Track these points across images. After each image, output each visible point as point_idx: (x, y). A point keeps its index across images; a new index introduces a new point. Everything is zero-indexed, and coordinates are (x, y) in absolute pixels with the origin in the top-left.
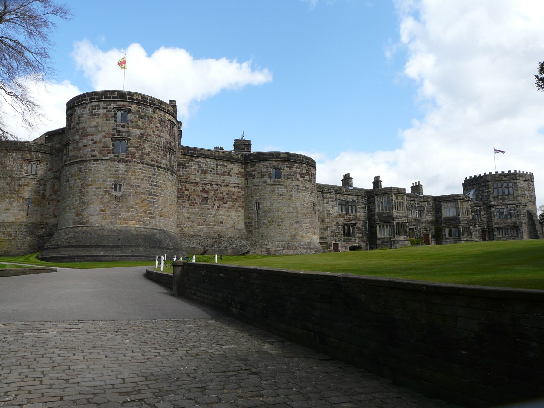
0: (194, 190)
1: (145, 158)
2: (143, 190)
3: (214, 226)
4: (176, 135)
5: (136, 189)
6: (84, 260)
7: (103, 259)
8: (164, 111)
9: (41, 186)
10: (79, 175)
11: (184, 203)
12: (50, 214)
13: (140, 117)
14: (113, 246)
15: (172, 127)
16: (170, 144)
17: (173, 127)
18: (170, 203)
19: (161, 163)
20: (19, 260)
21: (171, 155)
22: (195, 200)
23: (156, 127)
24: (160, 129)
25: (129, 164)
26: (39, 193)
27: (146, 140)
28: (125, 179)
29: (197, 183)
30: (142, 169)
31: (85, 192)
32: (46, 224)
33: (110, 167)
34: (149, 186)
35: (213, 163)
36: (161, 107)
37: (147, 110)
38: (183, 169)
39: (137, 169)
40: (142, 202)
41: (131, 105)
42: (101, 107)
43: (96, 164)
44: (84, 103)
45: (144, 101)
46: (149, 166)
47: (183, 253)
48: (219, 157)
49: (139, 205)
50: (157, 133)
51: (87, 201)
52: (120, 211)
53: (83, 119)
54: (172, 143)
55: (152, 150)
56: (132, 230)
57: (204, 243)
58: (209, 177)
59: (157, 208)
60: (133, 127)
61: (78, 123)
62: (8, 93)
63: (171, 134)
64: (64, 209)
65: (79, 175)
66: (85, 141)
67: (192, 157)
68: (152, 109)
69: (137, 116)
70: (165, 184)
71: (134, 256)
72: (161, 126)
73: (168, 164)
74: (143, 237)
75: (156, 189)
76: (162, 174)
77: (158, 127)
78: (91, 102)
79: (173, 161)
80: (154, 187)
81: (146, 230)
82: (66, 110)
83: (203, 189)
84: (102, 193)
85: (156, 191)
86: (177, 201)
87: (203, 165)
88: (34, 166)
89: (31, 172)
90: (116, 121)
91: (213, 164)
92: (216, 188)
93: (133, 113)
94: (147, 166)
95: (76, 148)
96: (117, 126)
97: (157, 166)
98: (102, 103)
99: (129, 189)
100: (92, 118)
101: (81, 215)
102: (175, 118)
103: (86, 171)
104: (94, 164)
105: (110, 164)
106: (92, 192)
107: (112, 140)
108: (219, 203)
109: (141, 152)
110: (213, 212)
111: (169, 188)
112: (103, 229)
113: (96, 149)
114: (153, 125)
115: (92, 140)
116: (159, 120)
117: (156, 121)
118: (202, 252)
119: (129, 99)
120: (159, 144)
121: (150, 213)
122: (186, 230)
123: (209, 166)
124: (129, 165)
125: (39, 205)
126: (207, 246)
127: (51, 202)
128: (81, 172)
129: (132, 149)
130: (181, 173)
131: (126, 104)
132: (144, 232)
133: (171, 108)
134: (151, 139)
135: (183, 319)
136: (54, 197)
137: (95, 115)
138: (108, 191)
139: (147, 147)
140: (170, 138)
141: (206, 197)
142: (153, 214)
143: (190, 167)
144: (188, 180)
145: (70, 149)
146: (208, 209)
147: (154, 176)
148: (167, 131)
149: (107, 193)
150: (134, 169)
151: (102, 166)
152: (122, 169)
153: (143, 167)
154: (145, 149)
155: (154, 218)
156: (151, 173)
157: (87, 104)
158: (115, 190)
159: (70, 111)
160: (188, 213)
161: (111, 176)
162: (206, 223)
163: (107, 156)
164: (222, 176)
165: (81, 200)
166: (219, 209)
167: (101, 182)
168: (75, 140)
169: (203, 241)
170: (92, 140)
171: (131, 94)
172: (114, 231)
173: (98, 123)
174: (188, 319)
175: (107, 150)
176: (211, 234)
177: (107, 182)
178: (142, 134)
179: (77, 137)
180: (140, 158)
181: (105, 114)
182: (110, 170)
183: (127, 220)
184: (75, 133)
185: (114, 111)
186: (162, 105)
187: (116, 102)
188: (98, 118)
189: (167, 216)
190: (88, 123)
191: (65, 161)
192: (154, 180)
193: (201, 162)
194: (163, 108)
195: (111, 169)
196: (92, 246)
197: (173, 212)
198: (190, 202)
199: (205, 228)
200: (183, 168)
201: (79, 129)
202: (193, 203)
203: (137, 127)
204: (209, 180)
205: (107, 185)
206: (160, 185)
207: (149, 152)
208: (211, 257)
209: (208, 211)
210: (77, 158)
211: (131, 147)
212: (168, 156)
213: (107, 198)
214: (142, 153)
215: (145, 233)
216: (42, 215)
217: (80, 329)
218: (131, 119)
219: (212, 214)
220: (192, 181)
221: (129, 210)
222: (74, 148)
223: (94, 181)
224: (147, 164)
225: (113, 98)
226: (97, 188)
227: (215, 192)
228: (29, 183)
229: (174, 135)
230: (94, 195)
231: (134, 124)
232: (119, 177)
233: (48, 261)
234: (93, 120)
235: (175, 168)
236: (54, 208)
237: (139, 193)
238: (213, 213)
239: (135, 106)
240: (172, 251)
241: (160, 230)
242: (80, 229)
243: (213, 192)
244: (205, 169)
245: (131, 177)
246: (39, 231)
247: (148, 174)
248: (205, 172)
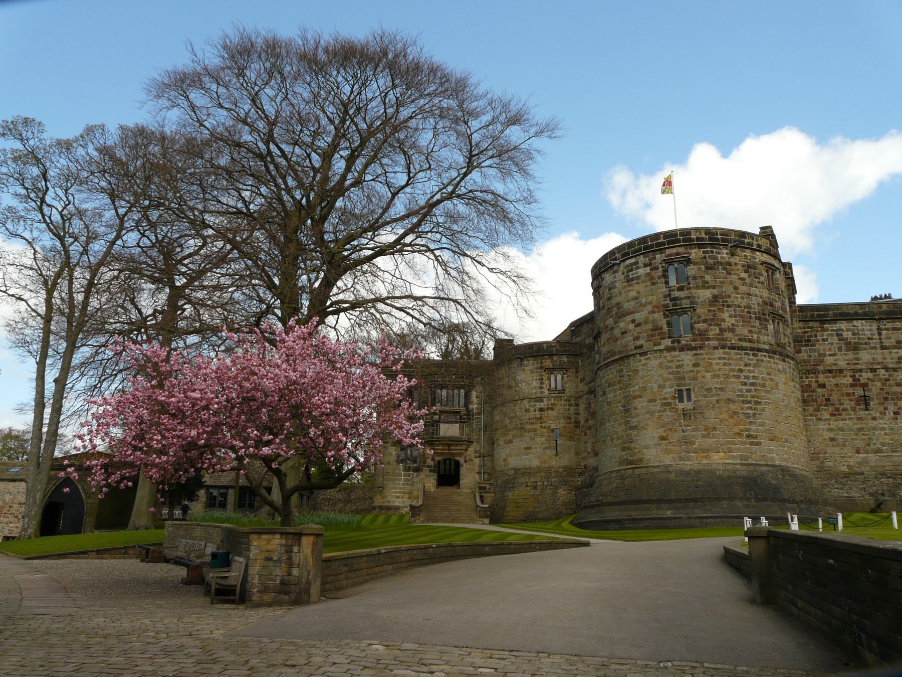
0: (837, 385)
1: (727, 338)
2: (730, 395)
3: (893, 452)
4: (783, 285)
5: (718, 395)
6: (641, 525)
7: (672, 524)
8: (751, 249)
9: (572, 408)
10: (619, 382)
11: (819, 411)
12: (589, 450)
13: (707, 268)
14: (688, 500)
15: (770, 274)
16: (771, 305)
17: (773, 273)
18: (788, 414)
19: (758, 342)
20: (548, 526)
21: (776, 324)
22: (841, 404)
23: (740, 279)
24: (747, 281)
25: (699, 352)
26: (570, 418)
27: (723, 306)
28: (695, 379)
29: (841, 371)
30: (725, 358)
31: (632, 410)
32: (585, 467)
33: (668, 362)
34: (741, 387)
35: (868, 328)
36: (743, 242)
37: (719, 253)
38: (808, 348)
39: (714, 359)
40: (731, 417)
41: (689, 250)
42: (641, 264)
43: (643, 360)
44: (614, 264)
45: (710, 239)
46: (736, 351)
47: (827, 510)
48: (881, 313)
49: (726, 423)
50: (743, 289)
51: (636, 424)
52: (693, 436)
53: (616, 290)
54: (776, 301)
55: (737, 321)
56: (719, 470)
57: (875, 488)
58: (865, 356)
59: (762, 425)
60: (697, 288)
61: (609, 299)
62: (492, 269)
63: (772, 287)
64: (604, 441)
65: (619, 382)
66: (622, 325)
67: (823, 322)
68: (727, 249)
69: (703, 267)
70: (772, 380)
71: (727, 517)
72: (749, 276)
73: (773, 343)
74: (740, 480)
75: (756, 390)
76: (762, 361)
77: (743, 279)
78: (624, 261)
79: (782, 336)
80: (750, 388)
81: (744, 467)
82: (591, 281)
83: (856, 380)
84: (658, 407)
85: (755, 394)
86: (804, 410)
87: (847, 335)
88: (559, 377)
89: (556, 387)
90: (667, 283)
91: (870, 330)
92: (884, 375)
93: (695, 264)
94: (732, 351)
95: (611, 338)
96: (670, 291)
97: (752, 349)
98: (642, 257)
99: (706, 396)
100: (629, 286)
101: (629, 448)
102: (777, 257)
103: (630, 373)
104: (640, 361)
105: (666, 357)
106: (643, 407)
107: (665, 316)
108: (896, 404)
109: (718, 328)
110: (886, 424)
111: (781, 386)
112: (667, 469)
113: (641, 335)
114: (734, 277)
115: (633, 321)
116: (743, 266)
117: (738, 269)
118: (873, 506)
119: (684, 240)
120: (750, 308)
121: (749, 436)
122: (831, 464)
123: (862, 335)
124: (700, 354)
125: (571, 438)
126: (883, 495)
127: (588, 432)
128: (622, 376)
129: (702, 324)
130: (804, 355)
131: (681, 250)
132: (743, 471)
133: (764, 240)
134: (733, 302)
135: (733, 667)
136: (591, 422)
137: (633, 279)
138: (669, 404)
139: (727, 318)
140: (771, 294)
141: (865, 396)
142: (756, 437)
143: (821, 342)
144: (821, 368)
145: (603, 342)
146: (874, 419)
147: (748, 368)
148: (763, 283)
149: (668, 408)
150: (709, 359)
151: (654, 362)
152: (688, 362)
153: (724, 353)
154: (725, 322)
155: (758, 444)
156: (742, 363)
157: (619, 264)
158: (681, 401)
159: (596, 282)
160: (830, 430)
161: (670, 376)
162: (872, 447)
163: (660, 344)
164: (894, 351)
165: (627, 423)
166: (899, 417)
167: (656, 390)
168: (607, 327)
169: (871, 483)
170: (633, 321)
171: (686, 232)
172: (687, 473)
173: (638, 292)
174: (747, 666)
175: (659, 334)
176: (887, 468)
177: (665, 388)
178: (715, 297)
179: (610, 321)
180: (718, 339)
181: (648, 275)
182: (668, 368)
183: (708, 453)
184: (607, 314)
185: (663, 267)
186: (745, 238)
187: (663, 251)
188: (638, 283)
189: (784, 440)
190: (623, 295)
191: (599, 363)
192: (749, 374)
193: (842, 330)
194: (749, 244)
195: (669, 365)
196: (650, 501)
197: (797, 430)
198: (831, 409)
199: (872, 457)
200: (807, 346)
201: (612, 308)
202: (837, 409)
203: (705, 285)
204: (866, 361)
205: (665, 393)
206: (762, 382)
207: (733, 325)
208: (885, 514)
209: (873, 424)
210: (614, 354)
211: (698, 322)
212: (770, 327)
213: (668, 416)
214: (720, 330)
215: (745, 473)
216: (577, 454)
217: (496, 669)
218: (694, 273)
219: (883, 429)
220: (830, 368)
221: (709, 433)
222: (608, 340)
223: (644, 389)
224: (733, 348)
225: (658, 245)
226: (651, 401)
227: (884, 384)
228: (554, 405)
229: (778, 288)
230: (648, 413)
231: (699, 281)
232: (684, 378)
233: (587, 529)
234: (630, 288)
235: (788, 348)
236: (593, 440)
237: (723, 402)
238: (886, 426)
239: (696, 250)
240: (803, 506)
241: (774, 466)
242: (630, 472)
243: (879, 385)
244: (853, 341)
245: (706, 374)
246: (576, 480)
247: (735, 365)
248: (855, 348)
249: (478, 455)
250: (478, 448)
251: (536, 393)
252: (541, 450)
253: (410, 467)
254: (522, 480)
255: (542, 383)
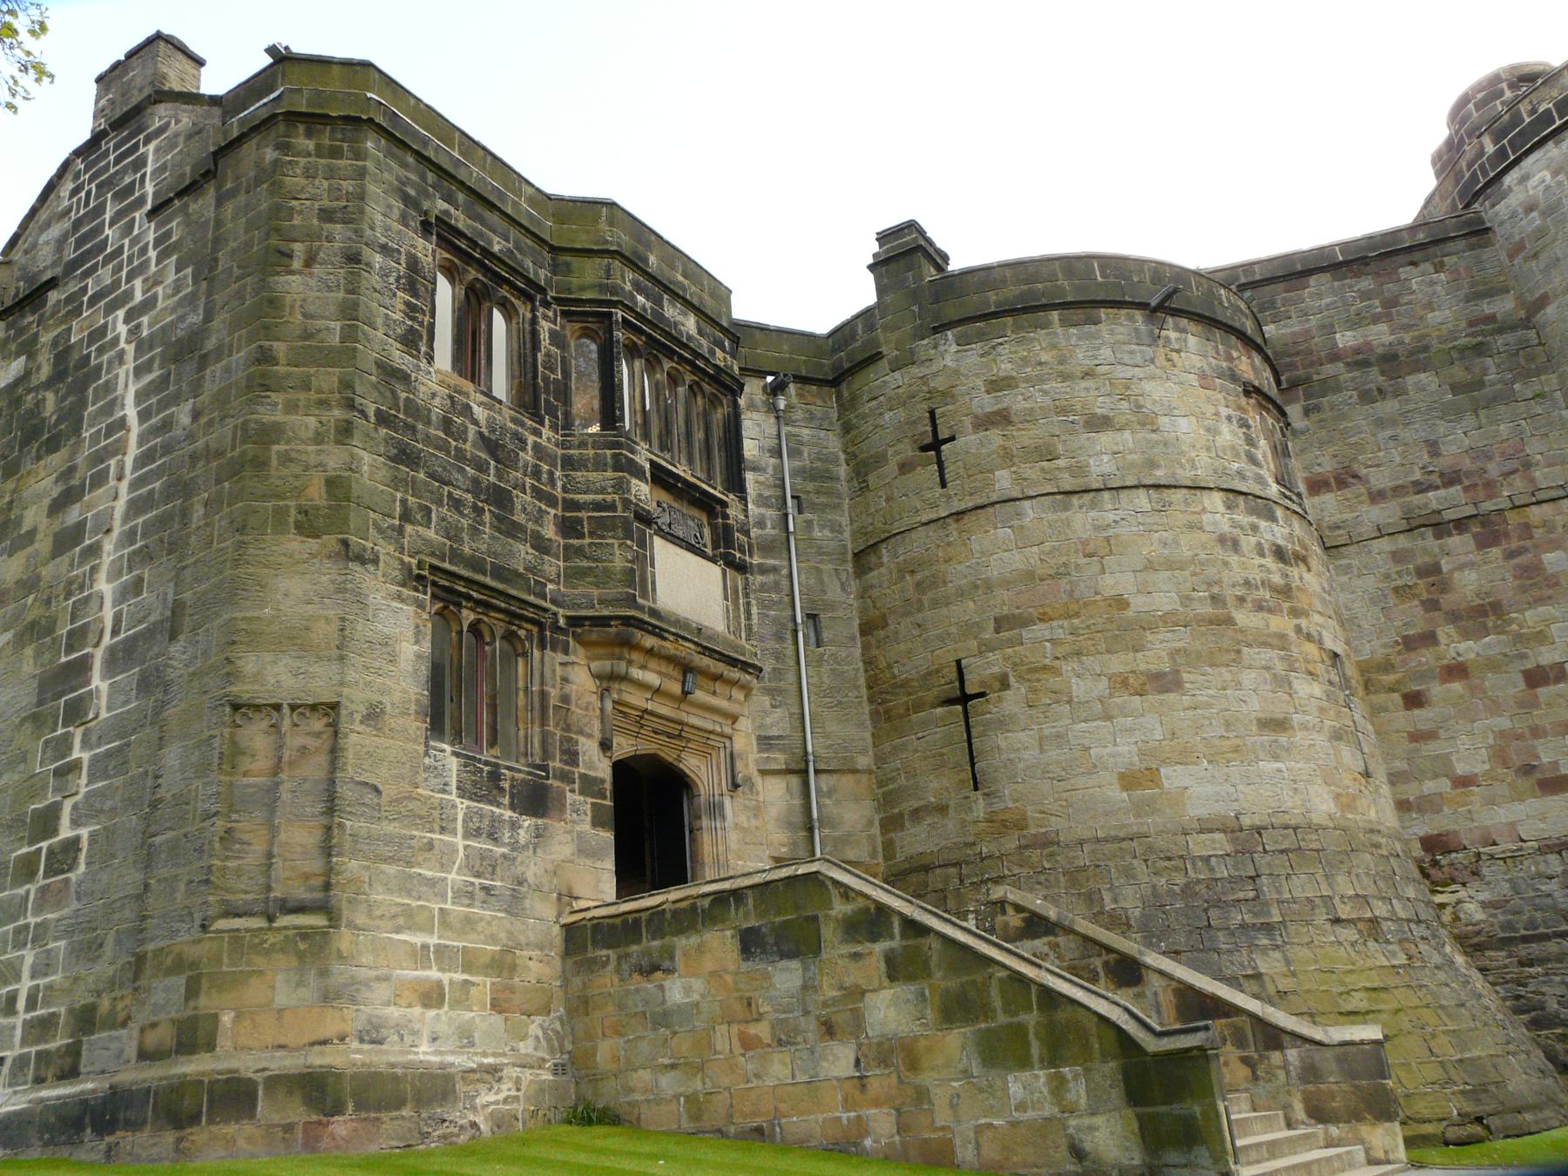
127: (1436, 690)
136: (1457, 646)
236: (1504, 723)
249: (779, 759)
250: (778, 722)
251: (1241, 475)
252: (1321, 740)
253: (495, 776)
254: (1301, 887)
255: (1250, 441)
